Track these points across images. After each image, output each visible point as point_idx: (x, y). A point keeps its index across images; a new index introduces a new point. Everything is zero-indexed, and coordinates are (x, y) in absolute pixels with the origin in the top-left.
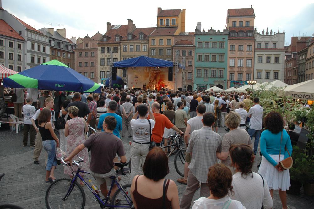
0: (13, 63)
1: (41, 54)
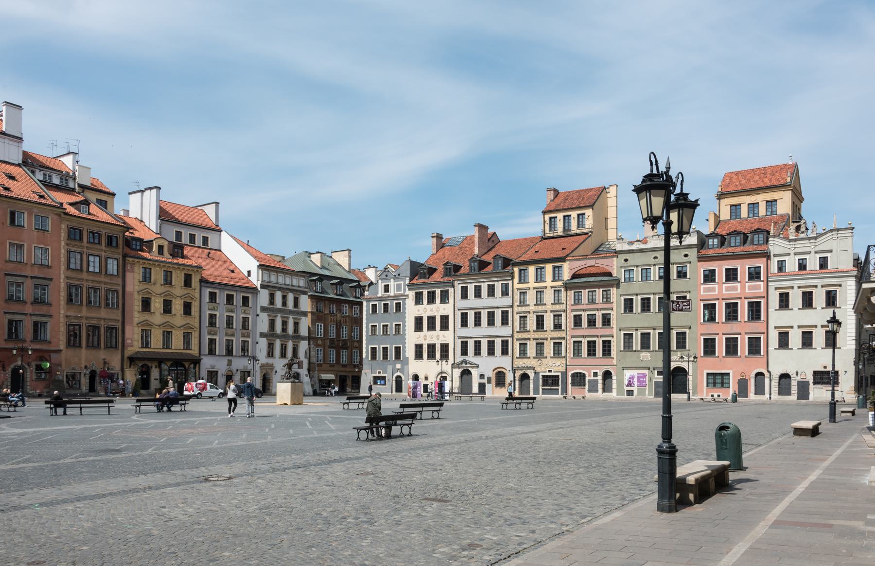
0: (233, 335)
1: (291, 312)
